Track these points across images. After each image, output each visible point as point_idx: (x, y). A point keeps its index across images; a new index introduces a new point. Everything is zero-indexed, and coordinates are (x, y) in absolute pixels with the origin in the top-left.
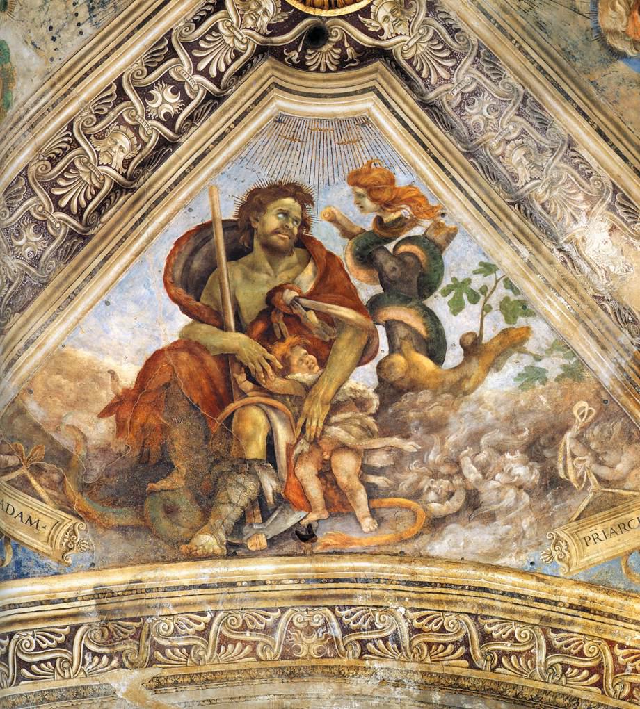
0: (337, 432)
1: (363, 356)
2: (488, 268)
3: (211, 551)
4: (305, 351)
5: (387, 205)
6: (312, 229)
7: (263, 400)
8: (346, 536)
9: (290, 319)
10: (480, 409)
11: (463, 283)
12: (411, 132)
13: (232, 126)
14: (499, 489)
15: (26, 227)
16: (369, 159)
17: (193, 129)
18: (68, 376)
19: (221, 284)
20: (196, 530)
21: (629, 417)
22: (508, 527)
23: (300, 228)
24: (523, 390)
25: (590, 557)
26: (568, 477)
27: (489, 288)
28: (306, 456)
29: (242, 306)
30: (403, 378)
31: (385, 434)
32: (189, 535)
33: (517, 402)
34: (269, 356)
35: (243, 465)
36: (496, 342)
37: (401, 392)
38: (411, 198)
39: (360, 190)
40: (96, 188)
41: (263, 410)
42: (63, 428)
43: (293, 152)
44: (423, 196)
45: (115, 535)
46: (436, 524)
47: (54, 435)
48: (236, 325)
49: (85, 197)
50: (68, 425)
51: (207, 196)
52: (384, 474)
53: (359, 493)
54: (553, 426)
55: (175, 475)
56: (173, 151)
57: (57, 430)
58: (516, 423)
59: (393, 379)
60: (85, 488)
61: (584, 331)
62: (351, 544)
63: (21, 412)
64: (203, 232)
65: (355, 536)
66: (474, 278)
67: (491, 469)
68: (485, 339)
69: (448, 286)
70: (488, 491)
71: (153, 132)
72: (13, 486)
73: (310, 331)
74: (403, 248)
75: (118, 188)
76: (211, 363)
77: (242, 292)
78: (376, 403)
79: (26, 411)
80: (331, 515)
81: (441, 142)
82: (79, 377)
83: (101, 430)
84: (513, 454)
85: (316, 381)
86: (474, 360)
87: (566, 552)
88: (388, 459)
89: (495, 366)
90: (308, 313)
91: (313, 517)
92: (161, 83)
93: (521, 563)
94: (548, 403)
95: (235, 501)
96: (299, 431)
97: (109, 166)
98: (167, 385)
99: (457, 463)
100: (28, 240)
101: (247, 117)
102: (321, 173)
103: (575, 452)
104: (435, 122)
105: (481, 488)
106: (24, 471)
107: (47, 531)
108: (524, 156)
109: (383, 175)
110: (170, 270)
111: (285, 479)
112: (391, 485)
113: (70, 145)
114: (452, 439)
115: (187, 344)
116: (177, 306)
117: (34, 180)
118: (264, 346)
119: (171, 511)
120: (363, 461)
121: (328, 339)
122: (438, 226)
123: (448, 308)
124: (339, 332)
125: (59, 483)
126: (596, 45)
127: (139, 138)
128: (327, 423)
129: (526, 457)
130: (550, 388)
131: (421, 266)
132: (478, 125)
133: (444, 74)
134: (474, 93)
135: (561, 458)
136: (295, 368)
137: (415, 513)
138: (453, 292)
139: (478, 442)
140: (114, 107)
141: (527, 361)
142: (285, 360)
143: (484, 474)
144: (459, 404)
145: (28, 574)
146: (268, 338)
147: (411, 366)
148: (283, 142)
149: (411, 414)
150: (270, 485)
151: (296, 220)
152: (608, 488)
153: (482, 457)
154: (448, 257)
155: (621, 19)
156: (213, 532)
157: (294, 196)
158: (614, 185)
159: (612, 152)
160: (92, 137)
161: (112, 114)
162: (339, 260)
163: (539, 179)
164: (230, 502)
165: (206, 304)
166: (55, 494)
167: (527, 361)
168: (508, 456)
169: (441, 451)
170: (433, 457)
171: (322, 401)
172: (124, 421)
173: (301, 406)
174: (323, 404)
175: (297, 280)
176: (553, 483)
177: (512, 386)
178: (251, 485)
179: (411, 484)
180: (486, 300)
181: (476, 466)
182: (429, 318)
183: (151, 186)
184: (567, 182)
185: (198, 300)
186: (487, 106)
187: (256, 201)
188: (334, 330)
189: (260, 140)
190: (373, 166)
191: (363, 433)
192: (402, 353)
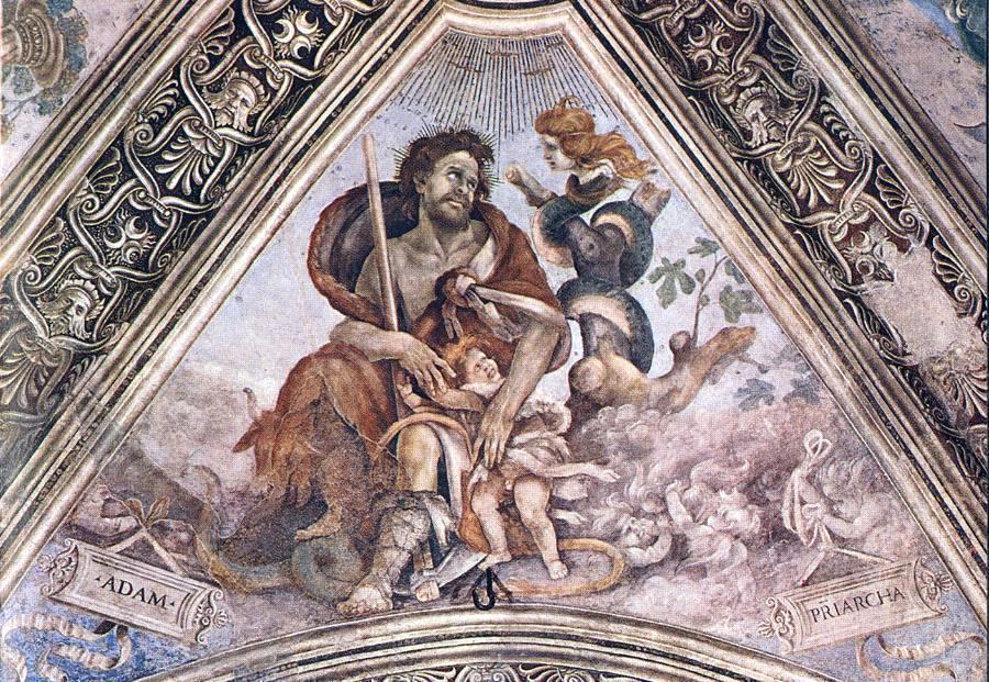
0: (517, 455)
1: (552, 360)
2: (706, 247)
3: (374, 606)
4: (483, 355)
5: (583, 160)
6: (491, 194)
7: (432, 417)
8: (533, 583)
9: (465, 314)
12: (617, 58)
13: (391, 50)
14: (711, 537)
15: (125, 223)
16: (563, 96)
17: (339, 57)
18: (192, 401)
19: (379, 268)
20: (357, 583)
21: (872, 457)
22: (722, 586)
23: (476, 194)
24: (744, 409)
25: (818, 637)
26: (795, 528)
27: (707, 272)
28: (484, 485)
29: (406, 298)
31: (578, 460)
32: (349, 590)
33: (736, 426)
34: (440, 362)
35: (410, 500)
36: (714, 345)
37: (598, 407)
38: (613, 149)
39: (551, 140)
40: (214, 158)
41: (433, 429)
42: (190, 470)
43: (468, 86)
44: (630, 148)
45: (259, 601)
46: (637, 573)
47: (179, 481)
48: (399, 323)
49: (201, 171)
50: (197, 467)
51: (359, 150)
52: (575, 509)
53: (547, 531)
54: (779, 461)
55: (328, 517)
56: (315, 88)
57: (183, 474)
58: (734, 453)
60: (220, 545)
61: (821, 335)
62: (537, 593)
63: (136, 456)
64: (356, 199)
65: (543, 584)
66: (689, 258)
67: (702, 510)
68: (701, 341)
69: (658, 269)
70: (698, 538)
71: (283, 76)
72: (130, 557)
73: (490, 331)
74: (603, 219)
75: (242, 150)
76: (369, 371)
77: (405, 280)
79: (143, 453)
80: (514, 558)
82: (208, 401)
83: (237, 469)
84: (729, 493)
85: (497, 392)
87: (790, 627)
88: (581, 491)
89: (709, 376)
90: (486, 306)
91: (492, 560)
92: (292, 9)
93: (733, 634)
95: (400, 544)
96: (476, 455)
97: (231, 127)
98: (315, 404)
100: (128, 239)
101: (407, 39)
102: (503, 116)
105: (689, 534)
106: (143, 534)
107: (175, 609)
108: (762, 109)
109: (579, 118)
110: (316, 252)
111: (460, 514)
112: (583, 523)
113: (177, 101)
114: (656, 469)
115: (338, 349)
116: (326, 300)
117: (131, 152)
118: (434, 350)
119: (324, 562)
120: (551, 492)
121: (511, 340)
122: (648, 189)
124: (525, 331)
125: (188, 544)
127: (266, 85)
128: (509, 444)
132: (705, 63)
134: (703, 19)
135: (787, 503)
136: (471, 377)
137: (612, 559)
138: (663, 278)
140: (231, 45)
142: (459, 366)
143: (694, 516)
144: (666, 425)
145: (154, 668)
146: (438, 340)
147: (610, 373)
148: (456, 72)
149: (609, 434)
150: (442, 522)
151: (471, 182)
153: (692, 494)
154: (658, 229)
156: (376, 583)
157: (470, 150)
158: (875, 153)
159: (877, 113)
160: (204, 90)
161: (229, 56)
162: (525, 236)
163: (779, 141)
164: (396, 546)
165: (362, 295)
166: (184, 558)
167: (750, 371)
168: (722, 494)
170: (635, 489)
171: (504, 417)
172: (266, 454)
173: (479, 423)
174: (506, 420)
175: (473, 264)
176: (777, 534)
177: (732, 403)
178: (419, 524)
179: (608, 523)
180: (703, 289)
181: (685, 506)
182: (633, 311)
183: (288, 137)
184: (817, 148)
185: (353, 292)
186: (716, 38)
187: (422, 155)
188: (519, 328)
189: (426, 68)
190: (567, 105)
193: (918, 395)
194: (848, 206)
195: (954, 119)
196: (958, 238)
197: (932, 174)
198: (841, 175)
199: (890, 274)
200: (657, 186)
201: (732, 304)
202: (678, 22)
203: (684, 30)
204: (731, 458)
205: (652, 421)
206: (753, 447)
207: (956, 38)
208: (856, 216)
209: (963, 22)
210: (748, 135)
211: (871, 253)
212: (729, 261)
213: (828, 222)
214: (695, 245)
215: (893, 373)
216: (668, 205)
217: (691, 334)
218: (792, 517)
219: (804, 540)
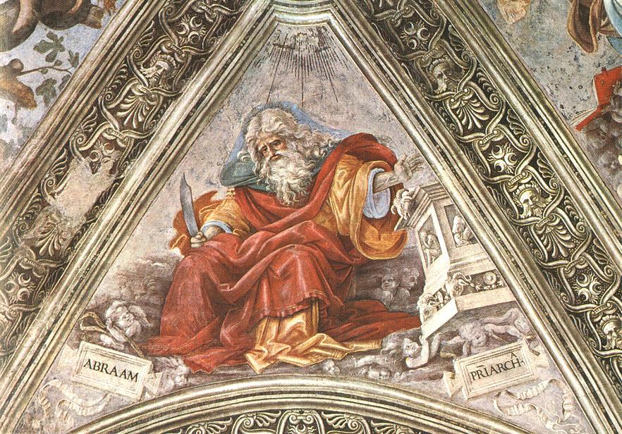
2: (74, 60)
27: (61, 66)
66: (66, 52)
68: (20, 78)
108: (164, 70)
132: (182, 30)
138: (52, 41)
141: (10, 114)
155: (270, 127)
163: (149, 85)
180: (51, 67)
184: (151, 107)
186: (197, 34)
193: (28, 210)
194: (126, 135)
196: (122, 195)
197: (152, 170)
198: (140, 124)
199: (96, 171)
201: (47, 88)
202: (201, 9)
203: (197, 13)
208: (121, 141)
209: (239, 161)
211: (104, 157)
212: (70, 76)
213: (112, 127)
215: (34, 191)
216: (93, 29)
217: (23, 71)
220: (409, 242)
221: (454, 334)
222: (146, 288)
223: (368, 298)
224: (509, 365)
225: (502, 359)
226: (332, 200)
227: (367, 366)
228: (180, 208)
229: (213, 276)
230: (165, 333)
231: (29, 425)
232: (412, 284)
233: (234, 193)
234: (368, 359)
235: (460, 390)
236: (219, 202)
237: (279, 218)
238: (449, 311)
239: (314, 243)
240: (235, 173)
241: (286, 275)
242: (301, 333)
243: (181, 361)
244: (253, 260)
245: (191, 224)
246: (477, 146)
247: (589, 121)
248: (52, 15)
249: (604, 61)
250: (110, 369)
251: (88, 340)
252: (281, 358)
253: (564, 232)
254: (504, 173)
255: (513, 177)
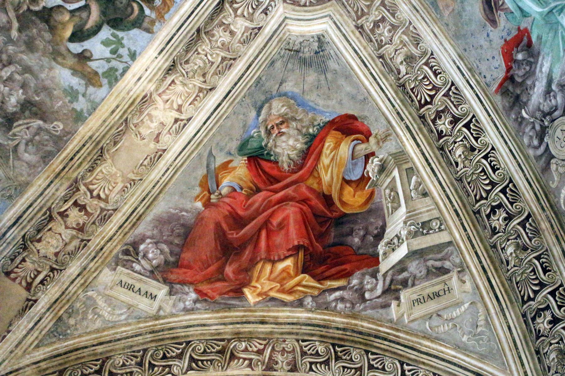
10: (47, 70)
11: (121, 44)
26: (15, 128)
30: (56, 21)
31: (18, 17)
33: (55, 90)
36: (89, 70)
37: (47, 22)
38: (166, 3)
44: (169, 10)
54: (44, 113)
58: (42, 92)
59: (54, 15)
67: (11, 83)
68: (90, 64)
78: (37, 8)
81: (203, 14)
84: (23, 94)
86: (76, 60)
89: (75, 72)
94: (58, 107)
99: (10, 63)
103: (31, 129)
104: (214, 8)
114: (25, 57)
122: (153, 22)
123: (104, 38)
126: (263, 98)
129: (22, 102)
130: (67, 106)
131: (126, 18)
133: (239, 12)
135: (25, 121)
138: (114, 39)
139: (26, 73)
141: (81, 89)
143: (6, 80)
144: (47, 57)
147: (64, 25)
149: (35, 31)
152: (13, 152)
153: (17, 77)
154: (135, 32)
155: (278, 111)
167: (81, 89)
168: (21, 91)
169: (15, 53)
170: (11, 48)
180: (113, 59)
181: (10, 75)
191: (16, 5)
192: (71, 18)
195: (214, 145)
200: (155, 27)
204: (39, 91)
205: (47, 49)
206: (48, 100)
207: (246, 136)
209: (253, 137)
210: (187, 62)
214: (133, 51)
218: (20, 125)
219: (11, 133)
220: (376, 198)
221: (403, 270)
222: (172, 231)
223: (341, 244)
224: (442, 293)
225: (436, 289)
226: (320, 166)
227: (336, 300)
228: (205, 172)
229: (224, 226)
230: (182, 267)
231: (66, 321)
232: (376, 232)
233: (247, 162)
234: (338, 294)
235: (403, 315)
236: (235, 168)
237: (278, 181)
238: (402, 252)
239: (305, 201)
240: (249, 147)
241: (282, 226)
242: (289, 273)
243: (191, 290)
244: (258, 213)
245: (212, 184)
246: (428, 116)
247: (501, 85)
248: (115, 20)
249: (504, 34)
250: (136, 289)
251: (124, 266)
252: (273, 294)
253: (485, 177)
254: (445, 135)
255: (451, 138)
